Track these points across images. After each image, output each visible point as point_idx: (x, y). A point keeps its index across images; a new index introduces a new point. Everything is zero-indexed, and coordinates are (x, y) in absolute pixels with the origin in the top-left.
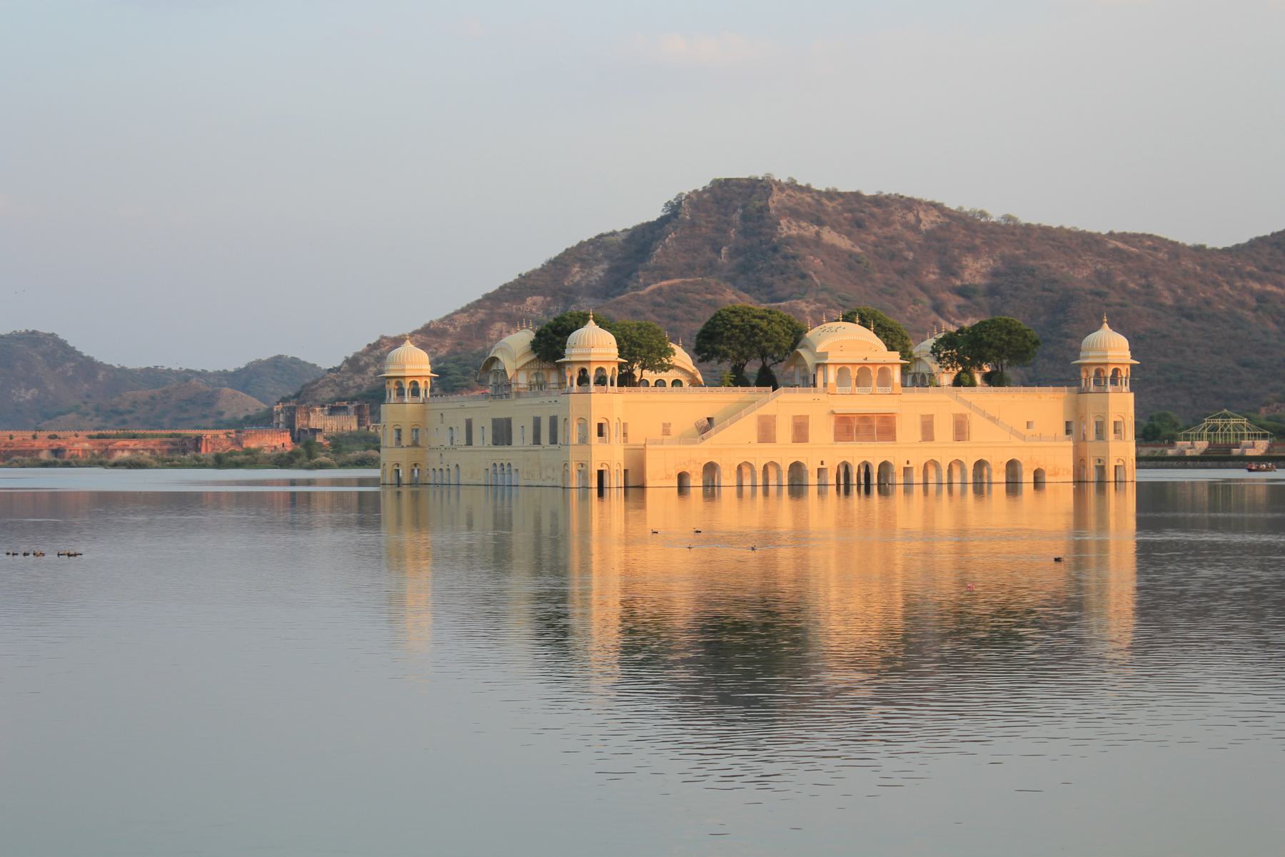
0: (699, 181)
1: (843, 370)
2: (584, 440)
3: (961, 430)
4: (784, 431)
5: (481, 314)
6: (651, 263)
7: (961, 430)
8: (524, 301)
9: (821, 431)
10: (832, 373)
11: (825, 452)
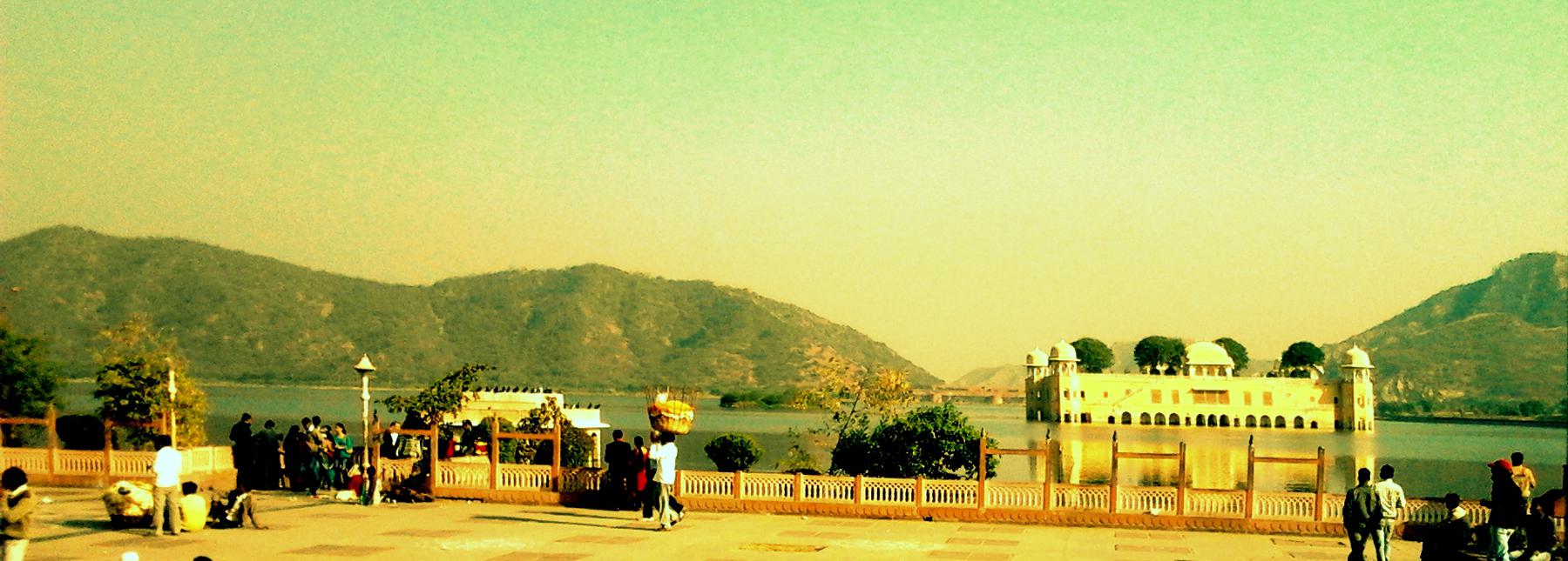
0: (1515, 254)
1: (1199, 368)
2: (1058, 399)
3: (1268, 399)
4: (1167, 398)
5: (1382, 332)
6: (1482, 304)
7: (1268, 399)
8: (1405, 324)
9: (1187, 400)
10: (1192, 370)
11: (1189, 408)
